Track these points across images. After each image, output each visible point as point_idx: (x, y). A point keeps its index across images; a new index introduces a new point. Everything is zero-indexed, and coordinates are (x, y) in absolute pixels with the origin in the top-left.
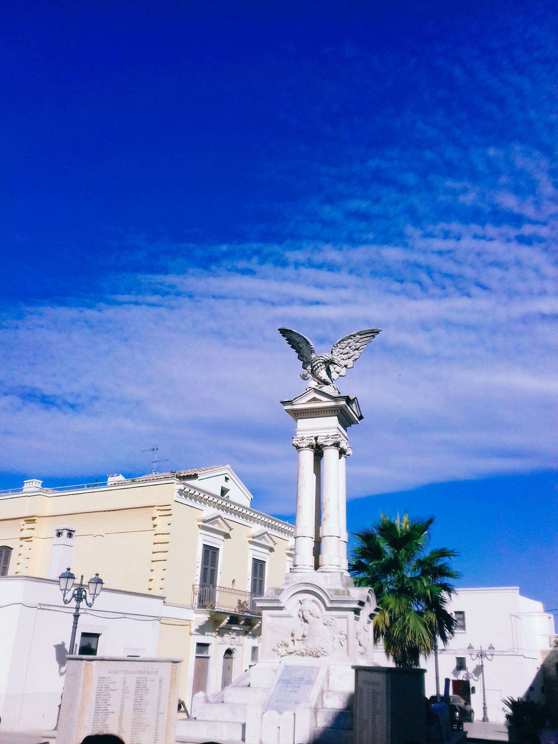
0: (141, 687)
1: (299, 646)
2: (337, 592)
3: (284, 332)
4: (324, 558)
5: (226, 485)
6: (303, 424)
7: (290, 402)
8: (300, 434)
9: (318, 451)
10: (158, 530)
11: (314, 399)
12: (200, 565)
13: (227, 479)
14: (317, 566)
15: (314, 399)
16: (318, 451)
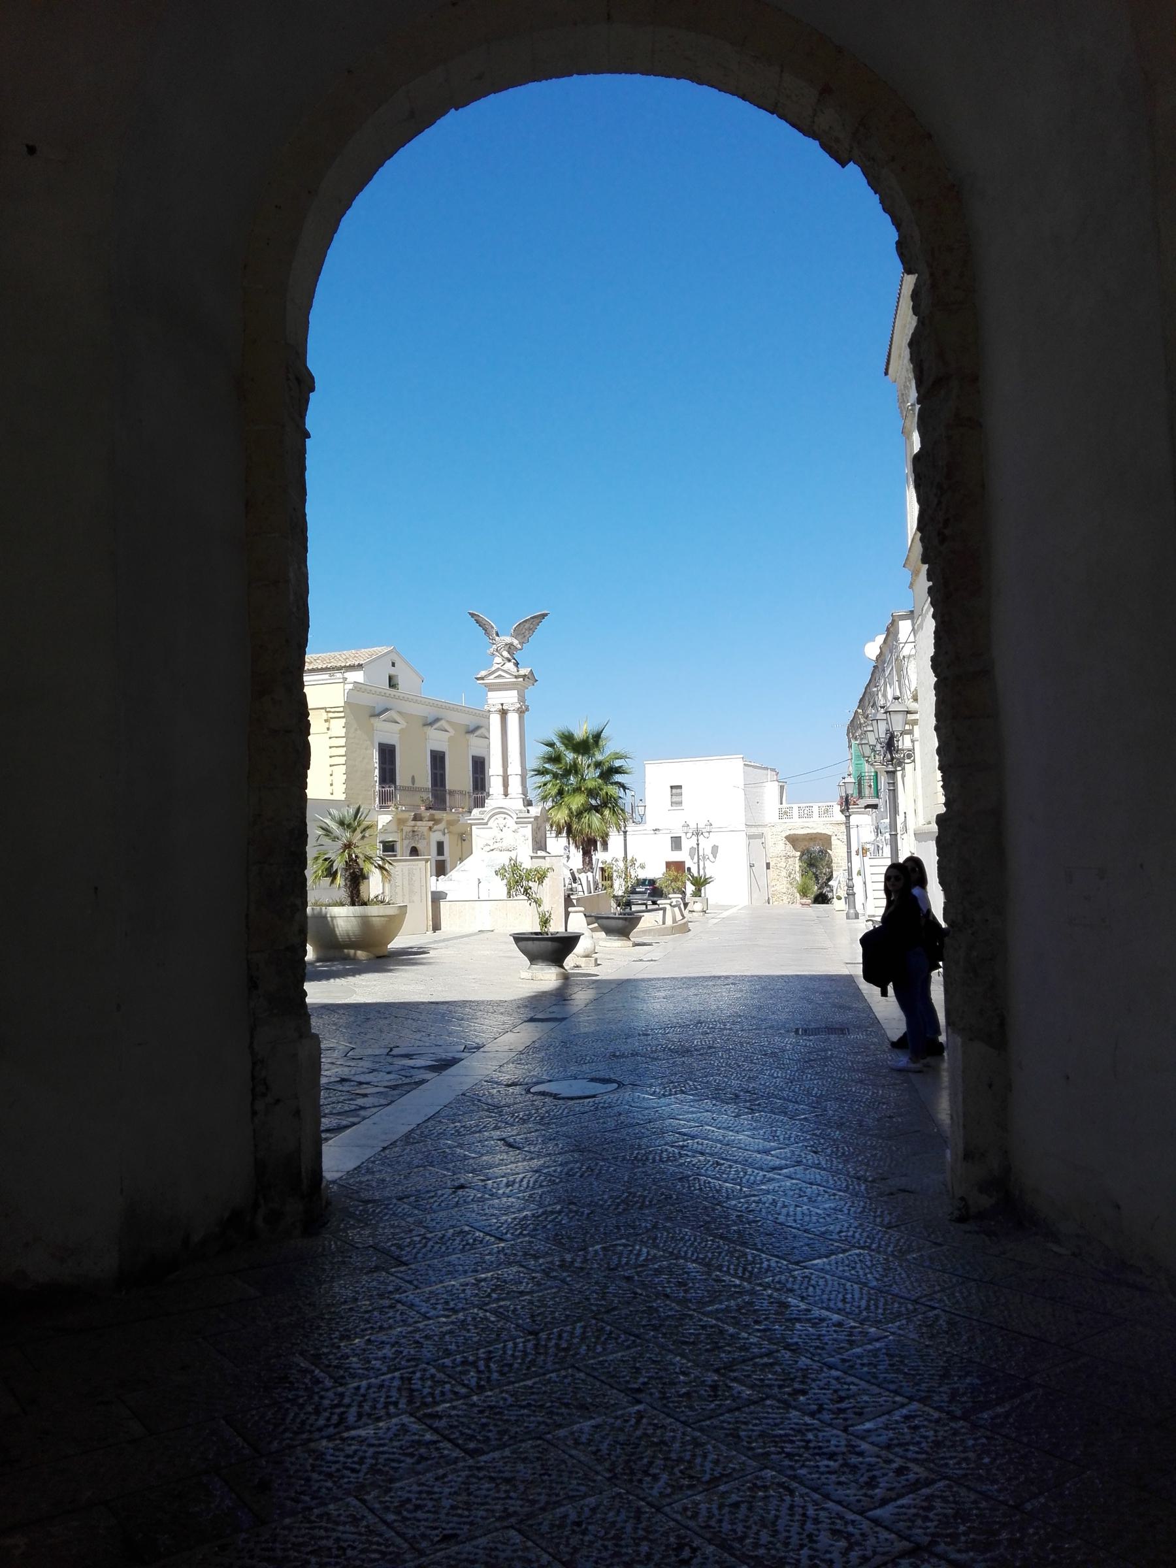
0: (410, 873)
1: (496, 846)
2: (521, 811)
3: (472, 615)
4: (510, 790)
5: (393, 671)
6: (490, 694)
7: (482, 678)
8: (490, 702)
9: (504, 713)
10: (330, 734)
11: (500, 676)
12: (377, 765)
13: (393, 665)
14: (506, 794)
15: (500, 676)
16: (504, 713)
